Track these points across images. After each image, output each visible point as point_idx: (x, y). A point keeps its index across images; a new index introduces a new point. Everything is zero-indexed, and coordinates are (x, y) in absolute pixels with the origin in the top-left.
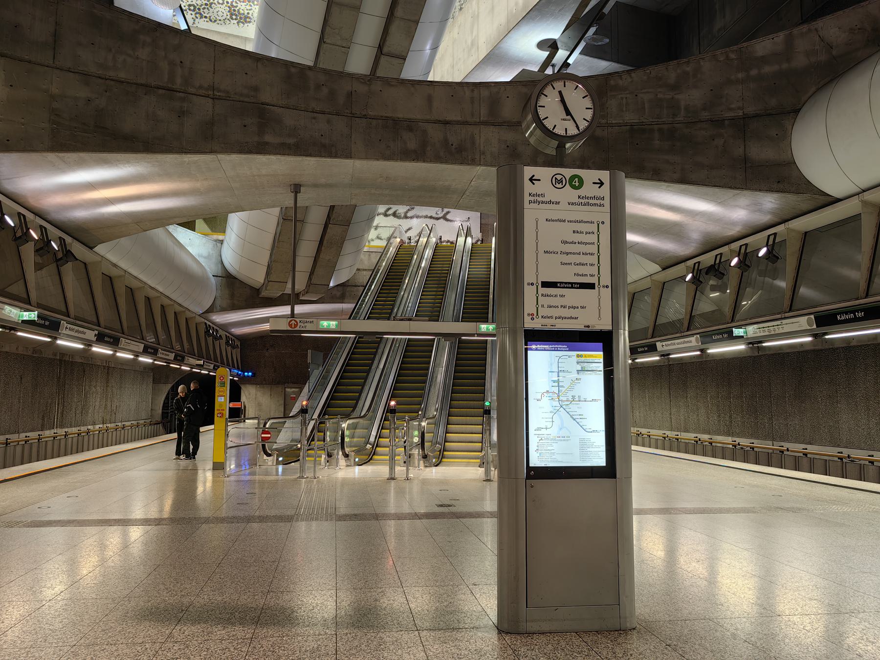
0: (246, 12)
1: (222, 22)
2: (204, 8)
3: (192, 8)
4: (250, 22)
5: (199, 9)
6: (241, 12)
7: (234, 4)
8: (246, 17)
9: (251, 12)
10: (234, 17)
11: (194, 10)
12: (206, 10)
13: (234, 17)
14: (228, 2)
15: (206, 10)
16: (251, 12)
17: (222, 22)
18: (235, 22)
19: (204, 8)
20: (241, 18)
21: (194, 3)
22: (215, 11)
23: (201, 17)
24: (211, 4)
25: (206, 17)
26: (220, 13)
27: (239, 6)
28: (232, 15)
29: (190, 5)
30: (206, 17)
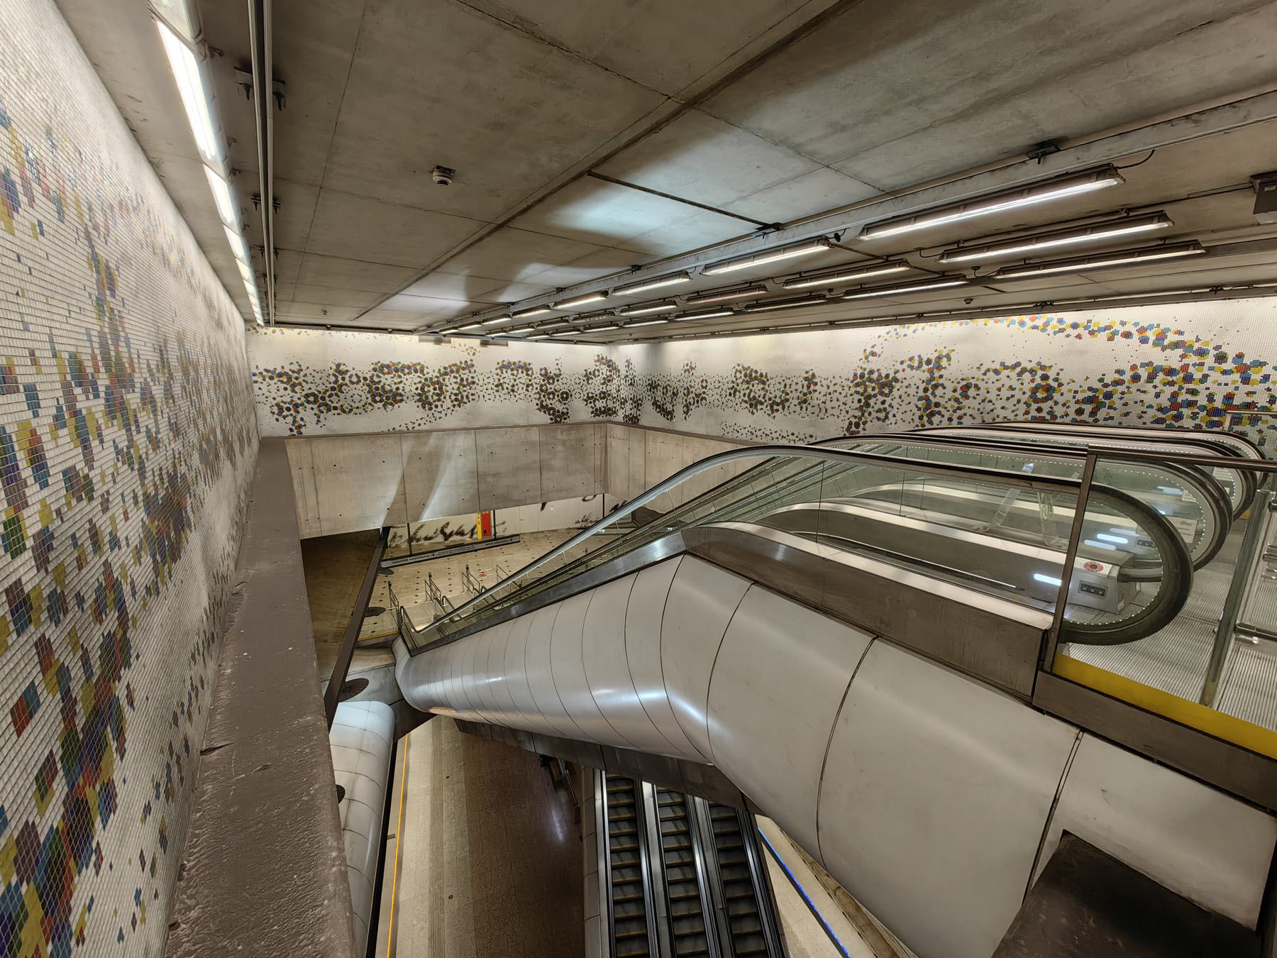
0: (394, 387)
1: (361, 410)
2: (330, 396)
3: (311, 399)
4: (401, 401)
5: (323, 398)
6: (388, 388)
7: (376, 379)
8: (395, 395)
9: (401, 386)
10: (378, 398)
11: (315, 402)
12: (334, 398)
13: (378, 398)
14: (365, 379)
15: (334, 398)
16: (401, 386)
17: (361, 410)
18: (380, 405)
19: (330, 396)
20: (388, 398)
21: (313, 391)
22: (348, 396)
23: (329, 410)
24: (341, 386)
25: (335, 408)
26: (356, 398)
27: (383, 380)
28: (373, 396)
29: (307, 396)
30: (335, 408)
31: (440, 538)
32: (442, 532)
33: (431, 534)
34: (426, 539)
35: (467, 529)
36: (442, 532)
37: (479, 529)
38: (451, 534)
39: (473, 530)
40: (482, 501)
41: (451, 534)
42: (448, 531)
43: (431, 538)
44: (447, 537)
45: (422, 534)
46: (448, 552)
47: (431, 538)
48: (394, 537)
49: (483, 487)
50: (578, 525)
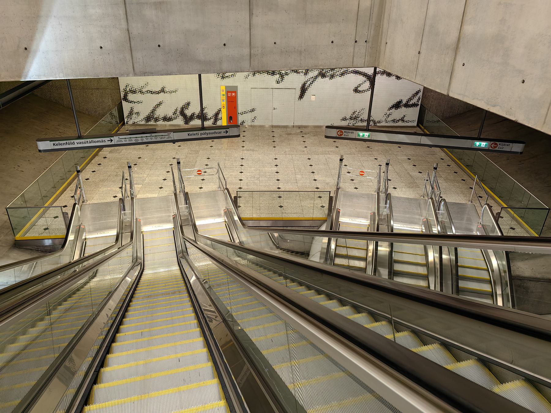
31: (179, 122)
32: (182, 113)
33: (170, 114)
34: (165, 119)
35: (210, 112)
36: (182, 113)
37: (224, 115)
38: (192, 117)
39: (217, 114)
40: (138, 55)
41: (192, 117)
42: (188, 113)
43: (170, 119)
44: (188, 119)
45: (160, 113)
46: (133, 138)
47: (170, 119)
48: (131, 113)
49: (136, 28)
50: (344, 124)
